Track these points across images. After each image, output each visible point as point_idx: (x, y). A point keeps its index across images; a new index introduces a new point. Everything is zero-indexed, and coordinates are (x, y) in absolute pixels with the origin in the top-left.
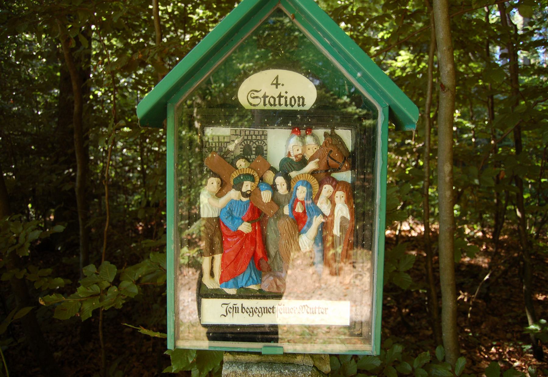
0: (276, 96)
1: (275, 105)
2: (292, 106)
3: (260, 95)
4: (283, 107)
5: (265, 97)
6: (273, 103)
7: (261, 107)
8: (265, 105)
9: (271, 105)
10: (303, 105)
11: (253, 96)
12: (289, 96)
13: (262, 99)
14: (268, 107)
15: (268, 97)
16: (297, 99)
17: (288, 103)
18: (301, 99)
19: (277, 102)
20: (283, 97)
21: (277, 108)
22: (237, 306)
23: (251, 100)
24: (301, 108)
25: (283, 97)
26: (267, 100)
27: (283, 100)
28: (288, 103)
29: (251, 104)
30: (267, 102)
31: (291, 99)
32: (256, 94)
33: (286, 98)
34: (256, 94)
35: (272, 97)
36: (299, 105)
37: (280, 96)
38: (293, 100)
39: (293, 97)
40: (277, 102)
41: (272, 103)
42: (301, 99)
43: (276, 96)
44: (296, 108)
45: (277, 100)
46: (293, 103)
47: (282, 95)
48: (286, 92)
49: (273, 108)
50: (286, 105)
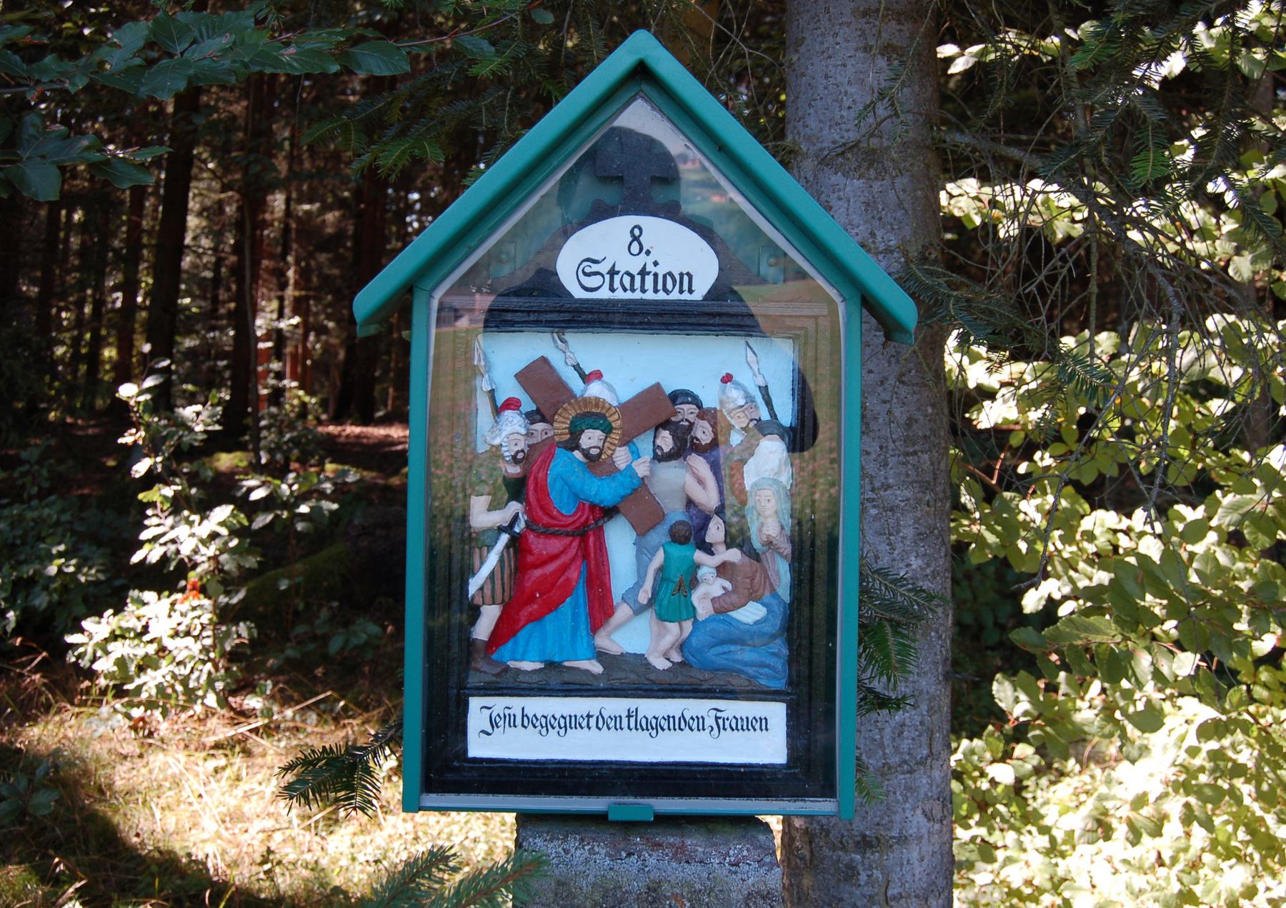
3: (604, 268)
4: (650, 295)
5: (613, 272)
6: (627, 285)
7: (604, 294)
9: (625, 290)
10: (691, 291)
12: (661, 271)
13: (607, 277)
14: (620, 295)
17: (660, 286)
18: (686, 278)
20: (649, 273)
21: (638, 295)
24: (686, 296)
25: (649, 273)
26: (617, 278)
27: (649, 280)
28: (660, 286)
30: (617, 284)
31: (665, 276)
32: (595, 268)
33: (656, 275)
34: (595, 268)
35: (628, 273)
36: (681, 292)
37: (643, 273)
39: (670, 274)
42: (686, 278)
46: (669, 286)
48: (656, 264)
49: (629, 295)
50: (656, 291)
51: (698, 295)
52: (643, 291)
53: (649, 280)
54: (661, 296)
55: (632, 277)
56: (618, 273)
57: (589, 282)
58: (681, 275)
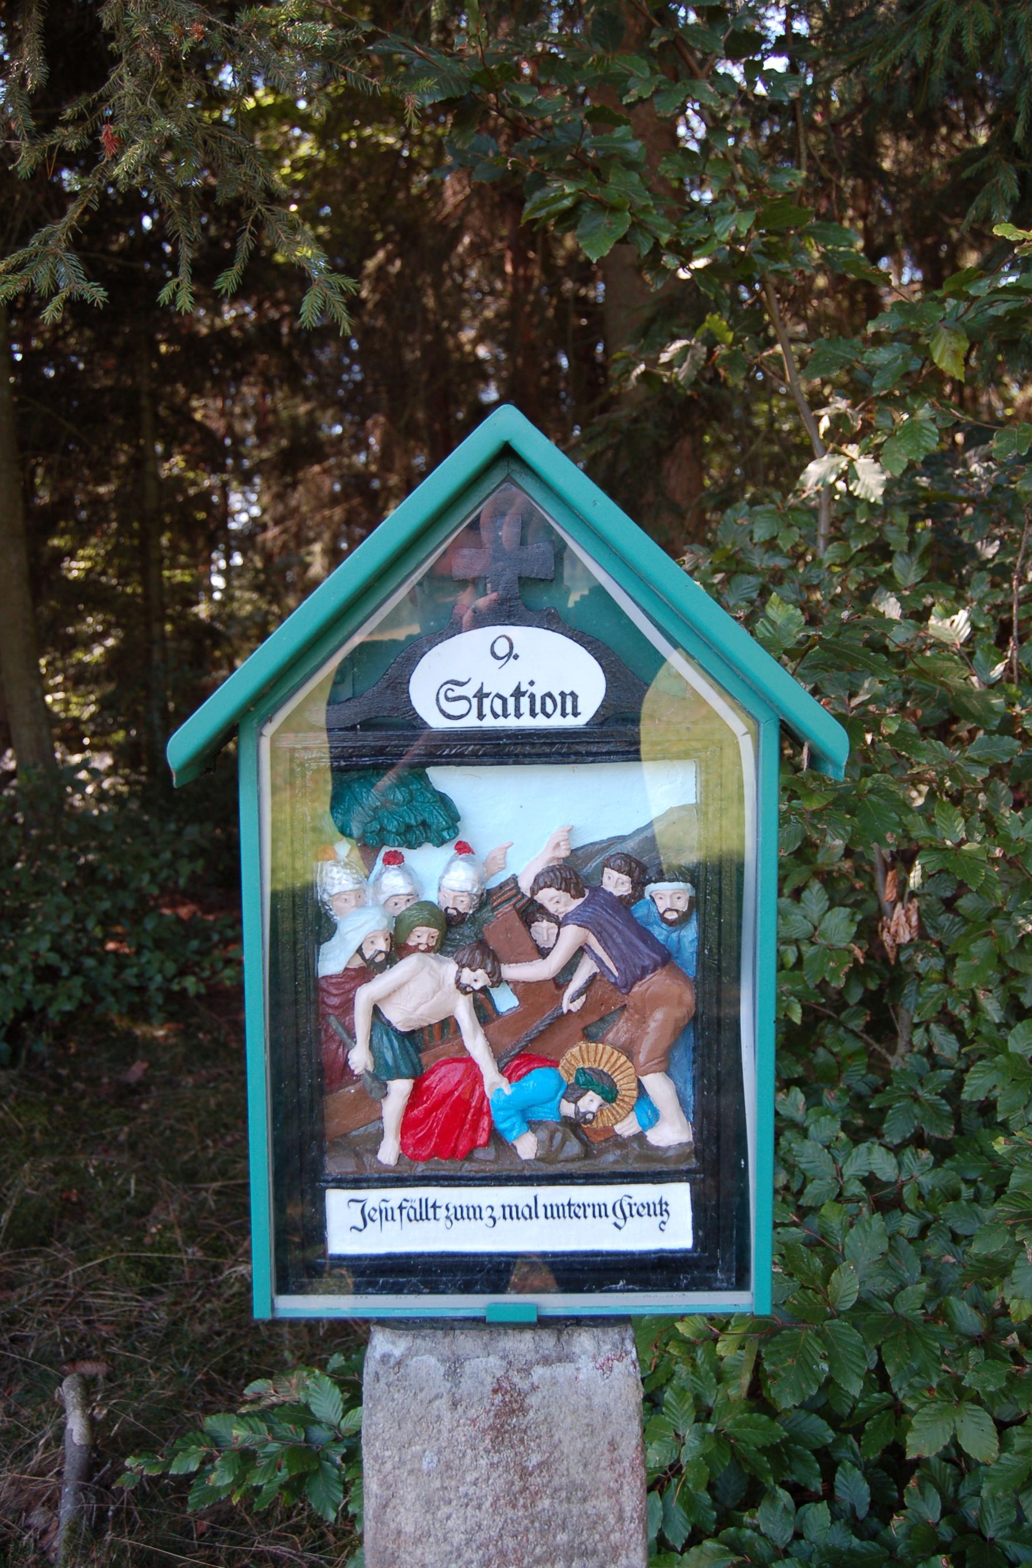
0: (507, 693)
1: (505, 715)
2: (548, 716)
3: (470, 691)
5: (481, 695)
6: (499, 710)
7: (471, 722)
8: (481, 716)
9: (496, 716)
11: (450, 694)
12: (539, 692)
13: (475, 702)
15: (487, 695)
16: (559, 699)
17: (538, 709)
19: (511, 708)
22: (389, 1205)
25: (524, 694)
26: (487, 702)
27: (525, 702)
28: (538, 709)
30: (486, 710)
31: (543, 698)
32: (459, 691)
33: (532, 697)
34: (459, 691)
35: (498, 696)
37: (518, 693)
38: (548, 701)
39: (550, 695)
40: (511, 708)
41: (498, 711)
43: (507, 693)
44: (556, 722)
45: (511, 702)
47: (523, 689)
48: (532, 683)
49: (501, 723)
50: (533, 714)
51: (581, 721)
53: (525, 702)
55: (504, 701)
56: (487, 695)
58: (563, 694)
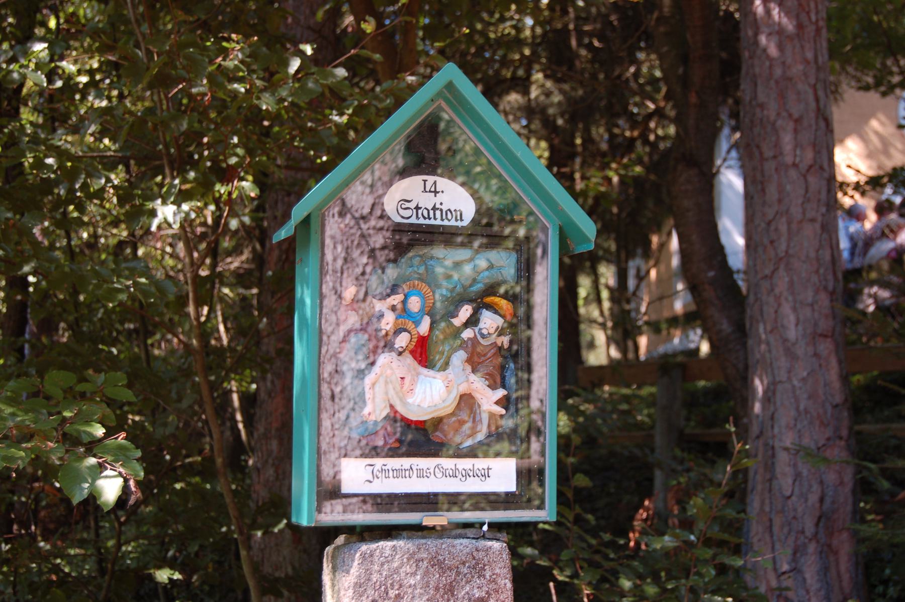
3: (412, 205)
4: (438, 222)
5: (417, 208)
6: (426, 215)
7: (413, 220)
8: (417, 217)
10: (461, 220)
11: (403, 206)
12: (444, 208)
14: (422, 221)
17: (444, 217)
21: (432, 222)
23: (402, 212)
24: (459, 224)
26: (420, 212)
27: (438, 213)
28: (444, 217)
29: (403, 217)
30: (420, 215)
32: (407, 205)
33: (441, 210)
34: (407, 205)
37: (434, 209)
39: (449, 210)
41: (426, 215)
43: (430, 208)
48: (441, 204)
49: (427, 222)
50: (442, 220)
52: (435, 219)
53: (438, 213)
54: (446, 223)
57: (402, 212)
